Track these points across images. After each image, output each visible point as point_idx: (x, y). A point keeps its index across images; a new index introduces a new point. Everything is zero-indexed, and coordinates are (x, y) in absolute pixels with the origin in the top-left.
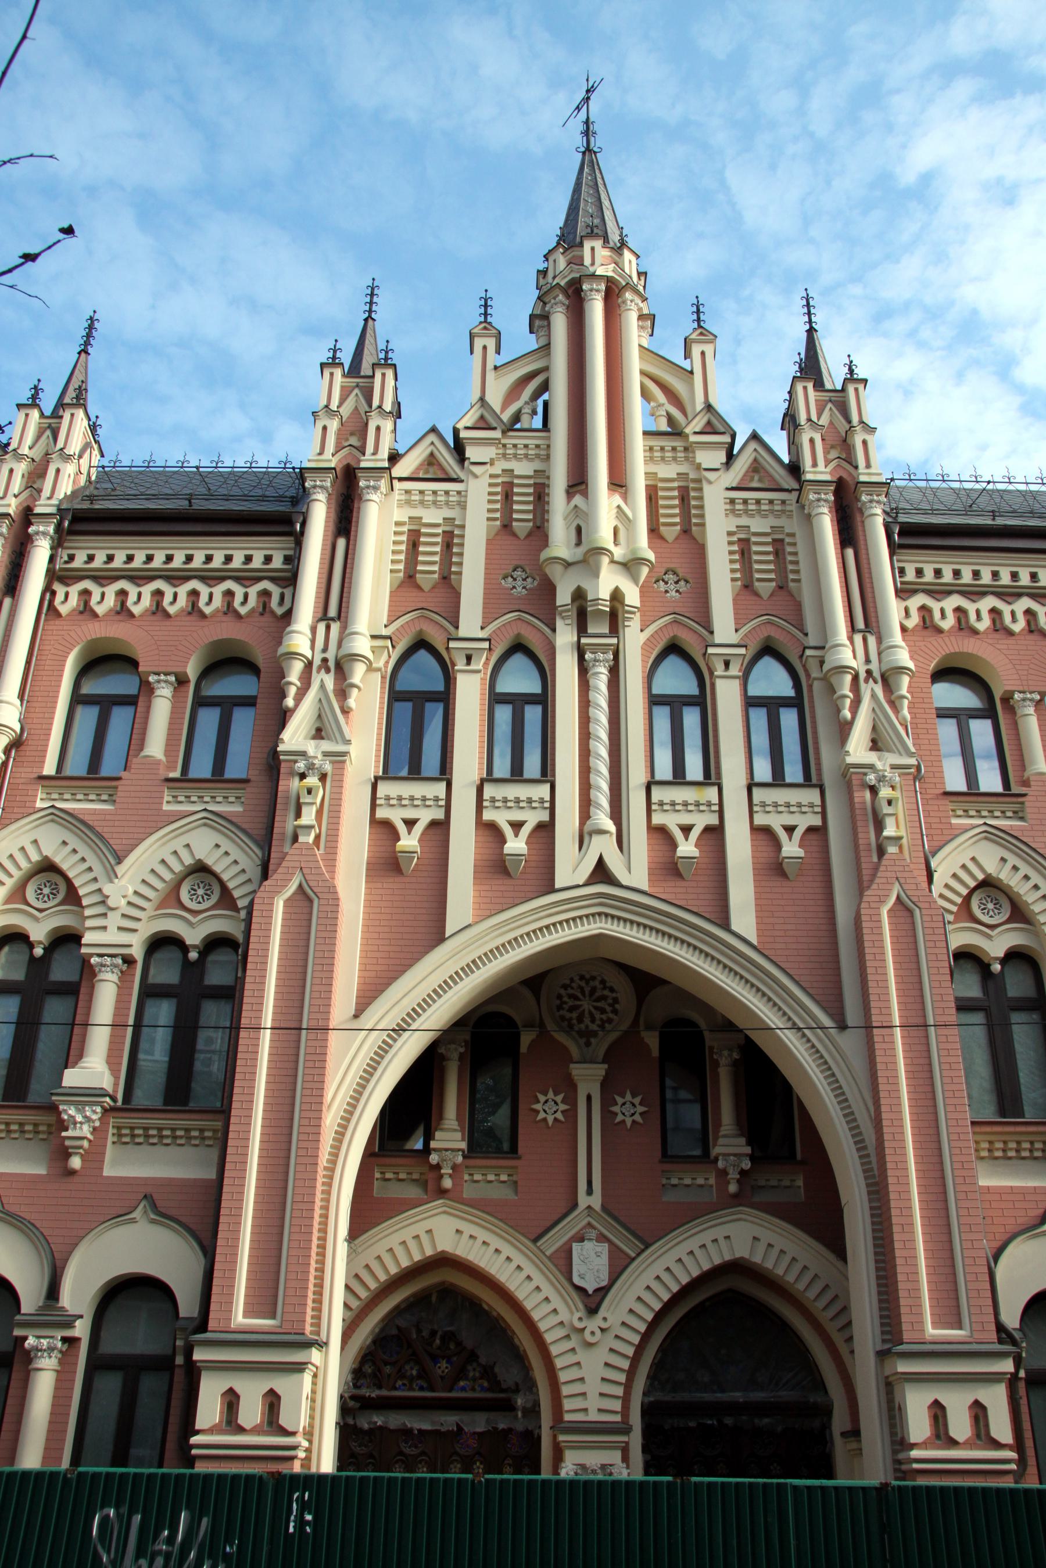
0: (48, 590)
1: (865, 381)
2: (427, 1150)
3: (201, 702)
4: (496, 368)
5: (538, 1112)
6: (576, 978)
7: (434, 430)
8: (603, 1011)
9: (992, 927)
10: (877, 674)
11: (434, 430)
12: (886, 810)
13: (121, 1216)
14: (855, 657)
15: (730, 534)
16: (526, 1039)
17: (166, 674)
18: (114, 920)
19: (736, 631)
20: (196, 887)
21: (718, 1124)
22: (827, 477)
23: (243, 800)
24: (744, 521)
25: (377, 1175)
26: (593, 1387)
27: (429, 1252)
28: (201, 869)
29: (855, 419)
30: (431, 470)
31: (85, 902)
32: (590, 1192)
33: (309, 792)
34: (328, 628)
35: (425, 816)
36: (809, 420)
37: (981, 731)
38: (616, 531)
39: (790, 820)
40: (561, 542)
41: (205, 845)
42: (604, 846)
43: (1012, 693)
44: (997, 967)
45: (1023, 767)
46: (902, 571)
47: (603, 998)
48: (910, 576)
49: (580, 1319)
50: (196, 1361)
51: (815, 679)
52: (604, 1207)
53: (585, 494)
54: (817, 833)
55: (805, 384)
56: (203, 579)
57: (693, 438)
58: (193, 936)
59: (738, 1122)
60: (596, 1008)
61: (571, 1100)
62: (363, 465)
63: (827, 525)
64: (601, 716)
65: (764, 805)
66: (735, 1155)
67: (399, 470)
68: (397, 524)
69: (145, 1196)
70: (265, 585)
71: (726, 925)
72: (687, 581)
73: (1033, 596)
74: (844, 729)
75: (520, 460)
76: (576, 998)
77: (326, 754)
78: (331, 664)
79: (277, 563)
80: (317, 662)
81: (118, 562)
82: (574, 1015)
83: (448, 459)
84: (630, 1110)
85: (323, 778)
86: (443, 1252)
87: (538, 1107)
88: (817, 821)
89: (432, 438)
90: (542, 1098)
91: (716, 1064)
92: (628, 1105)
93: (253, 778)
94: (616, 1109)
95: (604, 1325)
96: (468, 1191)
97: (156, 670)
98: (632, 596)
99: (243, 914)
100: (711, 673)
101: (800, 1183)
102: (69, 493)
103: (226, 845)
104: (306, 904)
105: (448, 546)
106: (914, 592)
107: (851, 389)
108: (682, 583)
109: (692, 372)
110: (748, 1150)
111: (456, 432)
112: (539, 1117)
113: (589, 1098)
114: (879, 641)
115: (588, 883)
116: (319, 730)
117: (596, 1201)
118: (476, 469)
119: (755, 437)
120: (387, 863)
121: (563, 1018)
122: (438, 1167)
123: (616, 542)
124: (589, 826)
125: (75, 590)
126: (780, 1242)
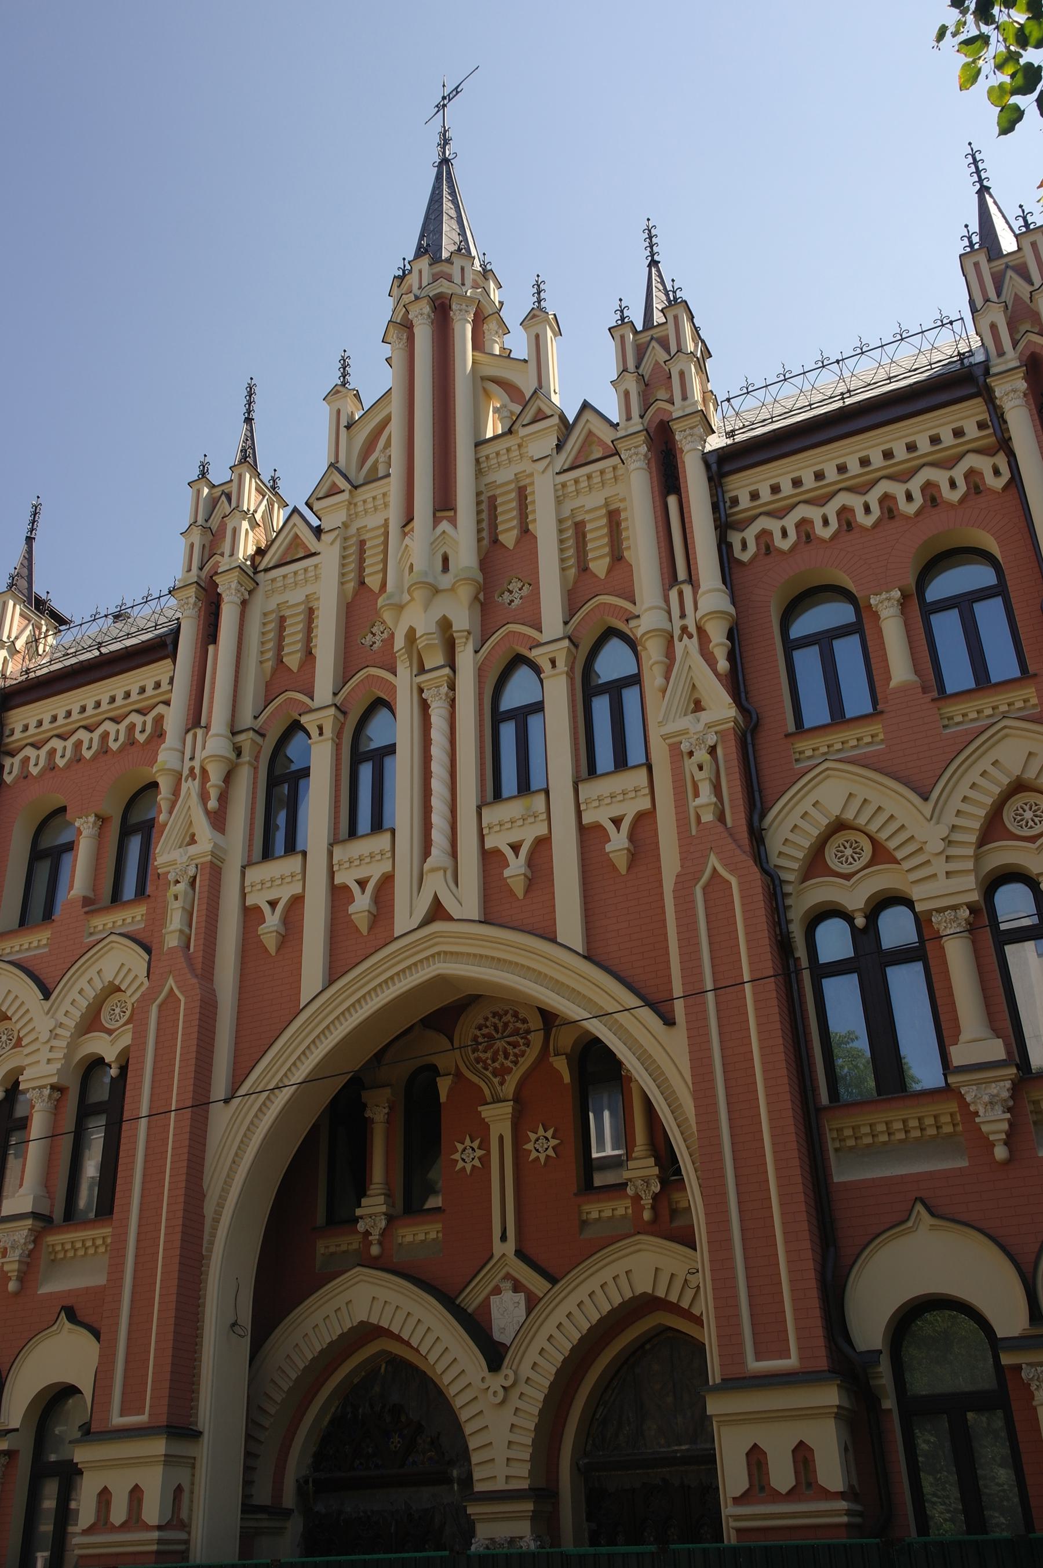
2: (356, 1220)
3: (126, 831)
6: (490, 1016)
7: (295, 510)
8: (515, 1045)
9: (847, 877)
10: (692, 629)
11: (295, 510)
12: (699, 775)
16: (444, 1086)
19: (566, 623)
22: (640, 427)
24: (577, 503)
29: (673, 349)
32: (504, 1238)
33: (176, 898)
38: (445, 560)
39: (615, 811)
44: (860, 922)
45: (889, 678)
46: (735, 501)
47: (516, 1032)
49: (483, 1379)
50: (77, 1464)
52: (519, 1253)
53: (412, 530)
60: (509, 1043)
61: (485, 1145)
67: (266, 561)
68: (265, 614)
69: (63, 1308)
71: (553, 940)
73: (888, 477)
78: (197, 771)
80: (186, 772)
82: (489, 1054)
83: (308, 537)
84: (542, 1145)
86: (362, 1323)
87: (457, 1156)
88: (645, 804)
90: (460, 1147)
92: (542, 1141)
94: (529, 1146)
95: (507, 1384)
110: (656, 1170)
113: (501, 1138)
117: (510, 1247)
119: (586, 406)
121: (478, 1060)
122: (367, 1233)
123: (446, 568)
124: (426, 867)
125: (17, 760)
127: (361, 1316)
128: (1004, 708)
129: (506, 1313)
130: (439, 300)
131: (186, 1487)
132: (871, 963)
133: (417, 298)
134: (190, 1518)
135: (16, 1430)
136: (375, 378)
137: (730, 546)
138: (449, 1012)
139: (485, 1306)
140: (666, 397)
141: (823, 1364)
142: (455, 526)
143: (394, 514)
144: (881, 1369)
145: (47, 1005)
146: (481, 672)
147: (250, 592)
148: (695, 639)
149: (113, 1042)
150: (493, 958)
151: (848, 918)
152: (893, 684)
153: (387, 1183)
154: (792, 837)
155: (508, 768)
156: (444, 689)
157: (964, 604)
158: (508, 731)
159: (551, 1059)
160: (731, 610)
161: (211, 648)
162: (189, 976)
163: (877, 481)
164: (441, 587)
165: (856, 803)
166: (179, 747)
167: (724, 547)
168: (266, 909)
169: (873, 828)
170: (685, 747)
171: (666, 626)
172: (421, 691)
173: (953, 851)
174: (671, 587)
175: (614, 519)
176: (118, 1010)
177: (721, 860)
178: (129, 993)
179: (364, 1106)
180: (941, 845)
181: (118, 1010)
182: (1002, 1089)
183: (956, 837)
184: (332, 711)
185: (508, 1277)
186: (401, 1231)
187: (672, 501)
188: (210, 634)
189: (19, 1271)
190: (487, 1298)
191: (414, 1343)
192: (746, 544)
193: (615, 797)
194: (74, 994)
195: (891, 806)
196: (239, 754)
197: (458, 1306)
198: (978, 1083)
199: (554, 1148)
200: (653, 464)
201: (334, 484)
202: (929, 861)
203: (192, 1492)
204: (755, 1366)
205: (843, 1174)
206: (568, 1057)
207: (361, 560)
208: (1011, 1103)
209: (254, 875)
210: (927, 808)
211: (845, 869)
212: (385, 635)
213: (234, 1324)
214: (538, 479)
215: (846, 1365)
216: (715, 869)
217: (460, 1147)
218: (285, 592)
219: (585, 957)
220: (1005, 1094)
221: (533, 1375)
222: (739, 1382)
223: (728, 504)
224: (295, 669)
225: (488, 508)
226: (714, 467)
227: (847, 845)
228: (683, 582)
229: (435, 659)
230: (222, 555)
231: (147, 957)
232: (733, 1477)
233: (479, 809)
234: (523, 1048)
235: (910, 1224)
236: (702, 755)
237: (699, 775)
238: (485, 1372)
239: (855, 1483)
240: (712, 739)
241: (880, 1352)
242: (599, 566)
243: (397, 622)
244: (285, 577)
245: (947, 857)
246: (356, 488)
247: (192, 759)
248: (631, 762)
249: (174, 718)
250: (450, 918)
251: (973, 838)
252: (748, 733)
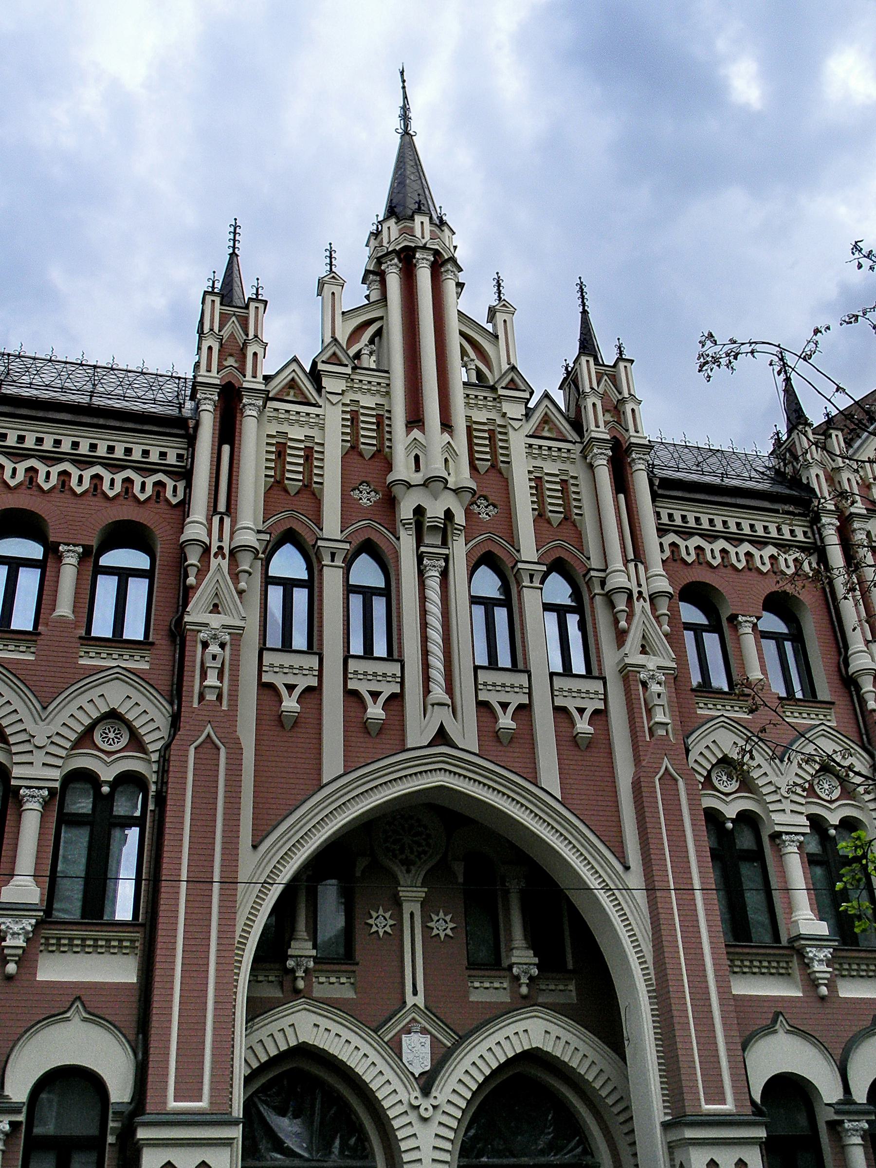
1: (632, 361)
2: (287, 957)
4: (343, 313)
5: (371, 926)
7: (295, 360)
8: (420, 845)
11: (295, 360)
13: (56, 1016)
14: (629, 580)
15: (530, 472)
17: (75, 545)
18: (39, 757)
20: (107, 731)
21: (510, 940)
23: (146, 659)
26: (427, 1154)
27: (293, 1043)
28: (113, 715)
30: (292, 392)
31: (12, 740)
32: (415, 993)
34: (221, 521)
35: (303, 683)
36: (592, 388)
37: (711, 641)
38: (446, 460)
40: (402, 469)
41: (116, 695)
42: (442, 716)
43: (736, 616)
48: (665, 520)
49: (416, 1098)
51: (596, 594)
55: (588, 358)
56: (105, 466)
57: (501, 392)
58: (107, 774)
59: (526, 938)
62: (245, 385)
63: (604, 475)
64: (434, 609)
65: (561, 690)
66: (526, 964)
68: (268, 436)
70: (160, 477)
72: (495, 506)
73: (751, 542)
74: (621, 636)
75: (364, 393)
77: (224, 627)
78: (226, 551)
79: (172, 459)
80: (214, 549)
81: (30, 443)
83: (307, 386)
84: (443, 925)
85: (222, 646)
87: (371, 921)
89: (294, 366)
91: (507, 892)
93: (157, 642)
96: (318, 991)
97: (66, 541)
98: (460, 518)
99: (155, 757)
100: (518, 583)
101: (572, 987)
103: (136, 697)
104: (215, 751)
105: (308, 458)
107: (622, 365)
108: (491, 507)
109: (497, 337)
110: (536, 960)
111: (314, 364)
112: (373, 930)
113: (412, 914)
114: (646, 570)
115: (430, 745)
116: (216, 606)
117: (420, 1000)
118: (335, 399)
120: (272, 720)
122: (293, 971)
126: (566, 1036)
130: (410, 245)
188: (228, 432)
201: (334, 354)
214: (511, 431)
216: (666, 768)
238: (418, 1093)
247: (221, 539)
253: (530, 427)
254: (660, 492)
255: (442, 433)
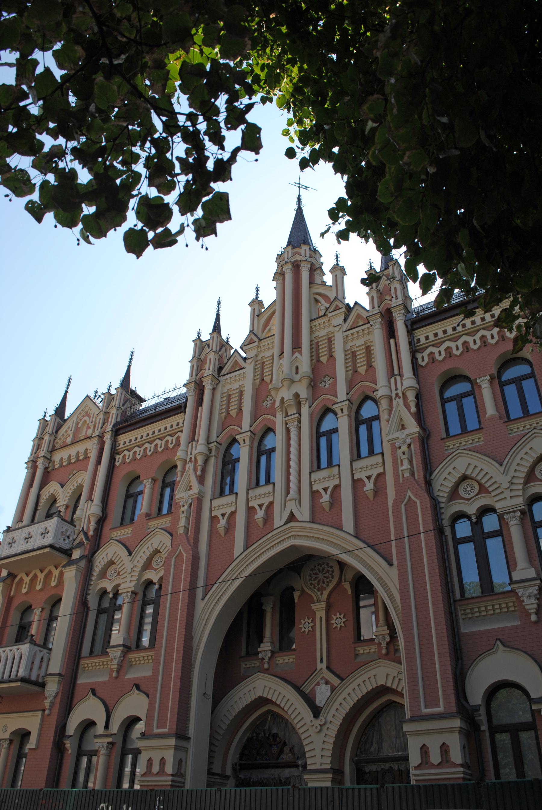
0: (112, 459)
3: (164, 486)
6: (317, 565)
10: (400, 394)
18: (129, 579)
19: (348, 394)
22: (378, 311)
24: (352, 344)
25: (243, 666)
31: (121, 573)
32: (321, 661)
33: (183, 512)
39: (368, 473)
46: (419, 340)
52: (328, 668)
54: (381, 476)
60: (325, 577)
68: (223, 394)
73: (483, 329)
76: (316, 574)
78: (193, 459)
82: (316, 582)
84: (338, 621)
87: (302, 626)
88: (381, 470)
90: (303, 622)
92: (339, 619)
94: (333, 622)
95: (322, 723)
102: (118, 420)
106: (427, 347)
110: (388, 632)
111: (241, 348)
113: (321, 618)
115: (285, 524)
117: (324, 665)
119: (356, 303)
121: (311, 584)
122: (263, 659)
123: (297, 373)
124: (288, 498)
125: (121, 456)
127: (259, 693)
128: (535, 425)
129: (322, 694)
131: (184, 760)
132: (479, 538)
133: (286, 262)
134: (185, 772)
135: (115, 734)
136: (269, 296)
137: (417, 359)
138: (299, 564)
139: (313, 689)
140: (389, 298)
141: (454, 709)
142: (301, 355)
143: (276, 351)
144: (480, 713)
145: (130, 558)
146: (311, 416)
147: (217, 385)
148: (402, 399)
149: (157, 574)
150: (316, 537)
151: (469, 517)
152: (487, 416)
153: (272, 637)
154: (443, 483)
155: (322, 456)
156: (296, 423)
157: (518, 381)
158: (323, 441)
159: (343, 584)
160: (417, 386)
161: (200, 408)
162: (188, 545)
163: (478, 330)
164: (295, 380)
165: (471, 468)
166: (186, 449)
167: (414, 359)
168: (220, 517)
169: (479, 478)
170: (397, 445)
171: (389, 394)
172: (286, 424)
173: (513, 487)
174: (392, 377)
175: (368, 350)
176: (159, 561)
177: (412, 493)
178: (163, 553)
179: (262, 604)
180: (508, 485)
181: (159, 561)
182: (534, 590)
183: (515, 481)
184: (249, 433)
185: (323, 677)
186: (278, 659)
187: (392, 341)
188: (200, 402)
189: (117, 668)
190: (314, 688)
191: (282, 706)
192: (423, 358)
193: (368, 467)
194: (141, 553)
195: (486, 469)
196: (210, 453)
197: (302, 690)
198: (524, 587)
199: (344, 622)
200: (384, 326)
201: (252, 339)
202: (503, 492)
203: (186, 762)
204: (425, 711)
205: (466, 629)
206: (350, 583)
207: (263, 370)
208: (538, 596)
209: (216, 503)
210: (502, 469)
211: (468, 496)
212: (272, 401)
213: (205, 694)
214: (336, 334)
215: (465, 711)
216: (410, 497)
217: (303, 622)
218: (230, 384)
219: (356, 537)
220: (535, 592)
221: (333, 720)
222: (417, 718)
223: (416, 342)
224: (235, 417)
225: (315, 347)
226: (409, 327)
227: (468, 486)
228: (397, 375)
229: (292, 411)
230: (205, 370)
231: (171, 538)
232: (415, 759)
233: (310, 473)
234: (331, 579)
235: (494, 650)
236: (404, 448)
237: (403, 457)
239: (468, 761)
240: (408, 441)
241: (481, 705)
242: (362, 370)
243: (276, 396)
244: (231, 378)
245: (511, 490)
246: (261, 340)
247: (191, 454)
248: (376, 452)
249: (184, 437)
250: (298, 521)
251: (522, 481)
252: (425, 439)
253: (346, 326)
254: (415, 327)
255: (293, 353)
